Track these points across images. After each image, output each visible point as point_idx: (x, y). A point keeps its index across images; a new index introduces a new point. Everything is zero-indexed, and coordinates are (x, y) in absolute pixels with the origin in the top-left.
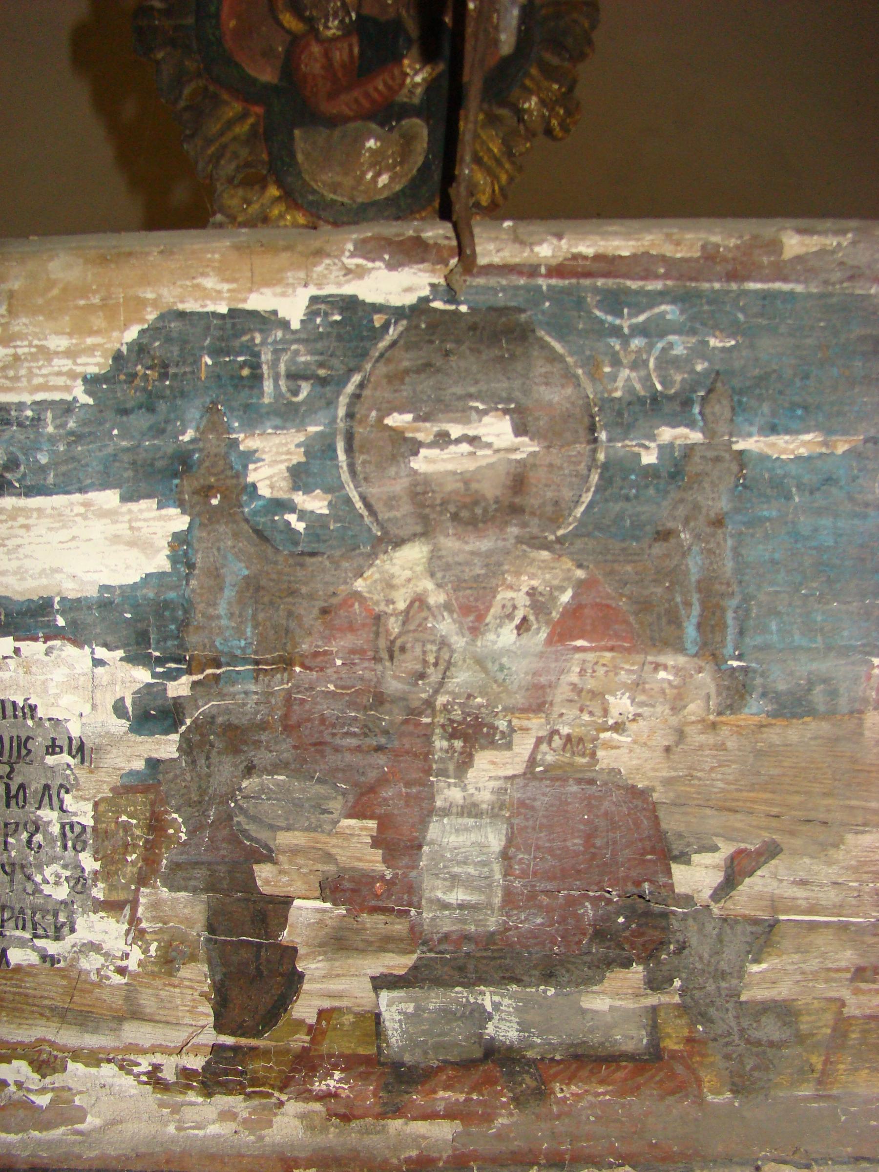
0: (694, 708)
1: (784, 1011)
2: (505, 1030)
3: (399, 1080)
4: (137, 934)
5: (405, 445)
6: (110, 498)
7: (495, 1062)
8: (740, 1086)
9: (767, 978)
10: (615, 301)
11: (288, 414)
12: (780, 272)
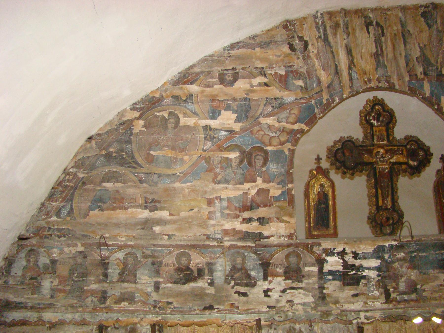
0: (417, 274)
1: (426, 297)
2: (406, 298)
3: (399, 302)
4: (379, 292)
5: (396, 255)
6: (375, 259)
7: (406, 301)
8: (423, 302)
9: (425, 294)
10: (410, 244)
11: (387, 253)
12: (422, 241)
